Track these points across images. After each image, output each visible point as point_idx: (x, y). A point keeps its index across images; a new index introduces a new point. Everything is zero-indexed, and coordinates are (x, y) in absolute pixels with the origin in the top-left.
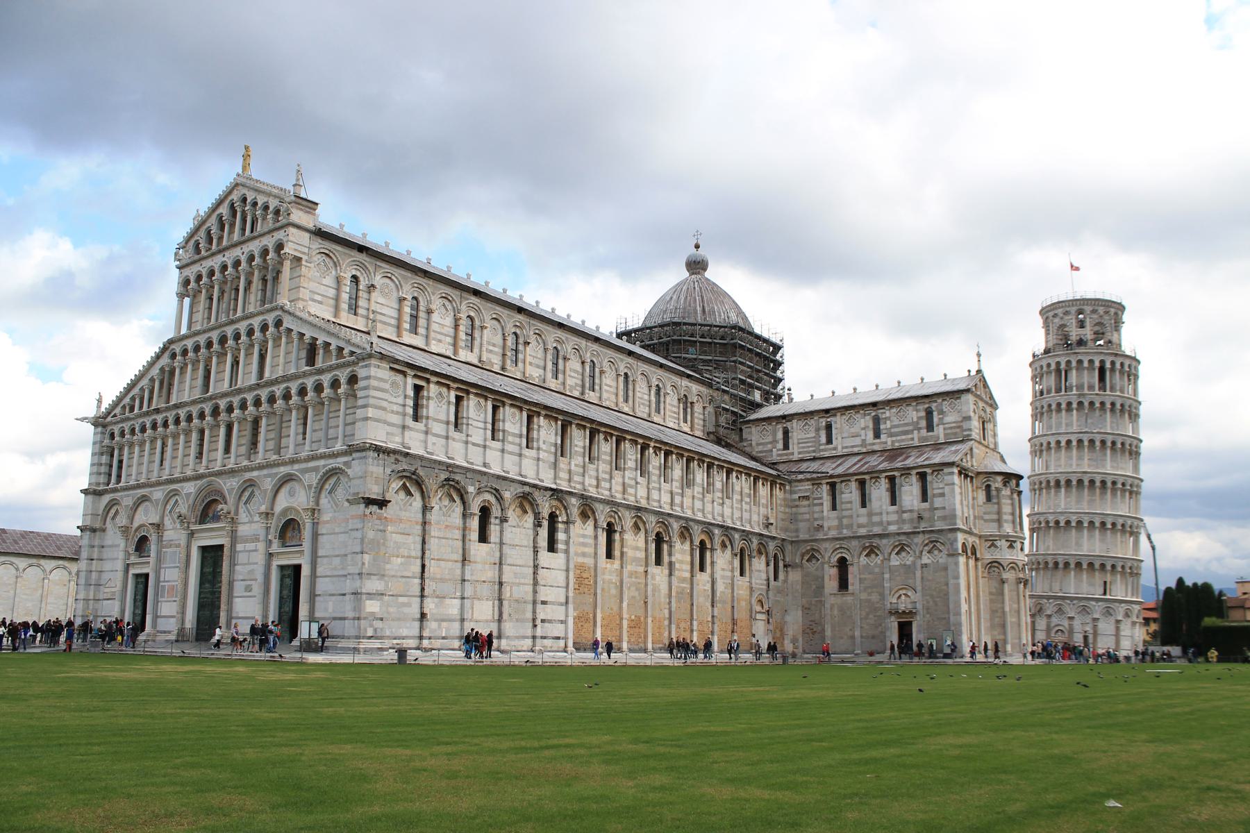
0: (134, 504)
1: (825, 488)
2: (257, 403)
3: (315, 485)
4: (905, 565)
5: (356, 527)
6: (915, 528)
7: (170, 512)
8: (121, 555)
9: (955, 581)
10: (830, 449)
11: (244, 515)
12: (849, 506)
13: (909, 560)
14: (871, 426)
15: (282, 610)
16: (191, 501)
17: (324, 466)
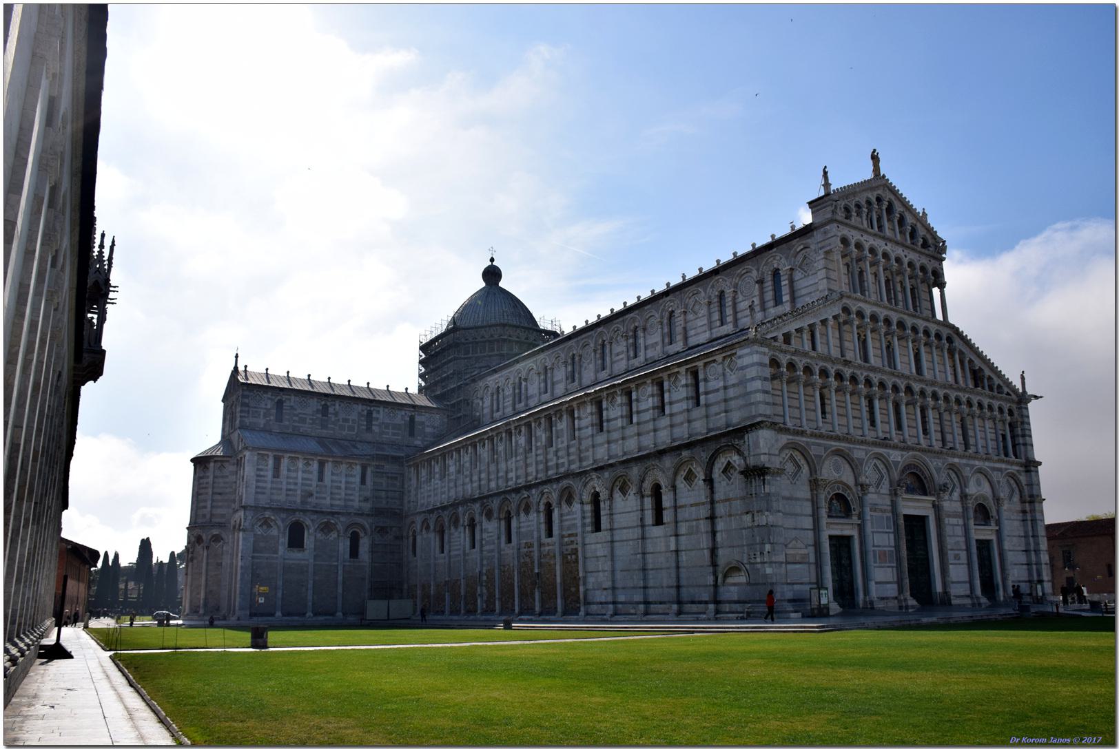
17: (1006, 469)
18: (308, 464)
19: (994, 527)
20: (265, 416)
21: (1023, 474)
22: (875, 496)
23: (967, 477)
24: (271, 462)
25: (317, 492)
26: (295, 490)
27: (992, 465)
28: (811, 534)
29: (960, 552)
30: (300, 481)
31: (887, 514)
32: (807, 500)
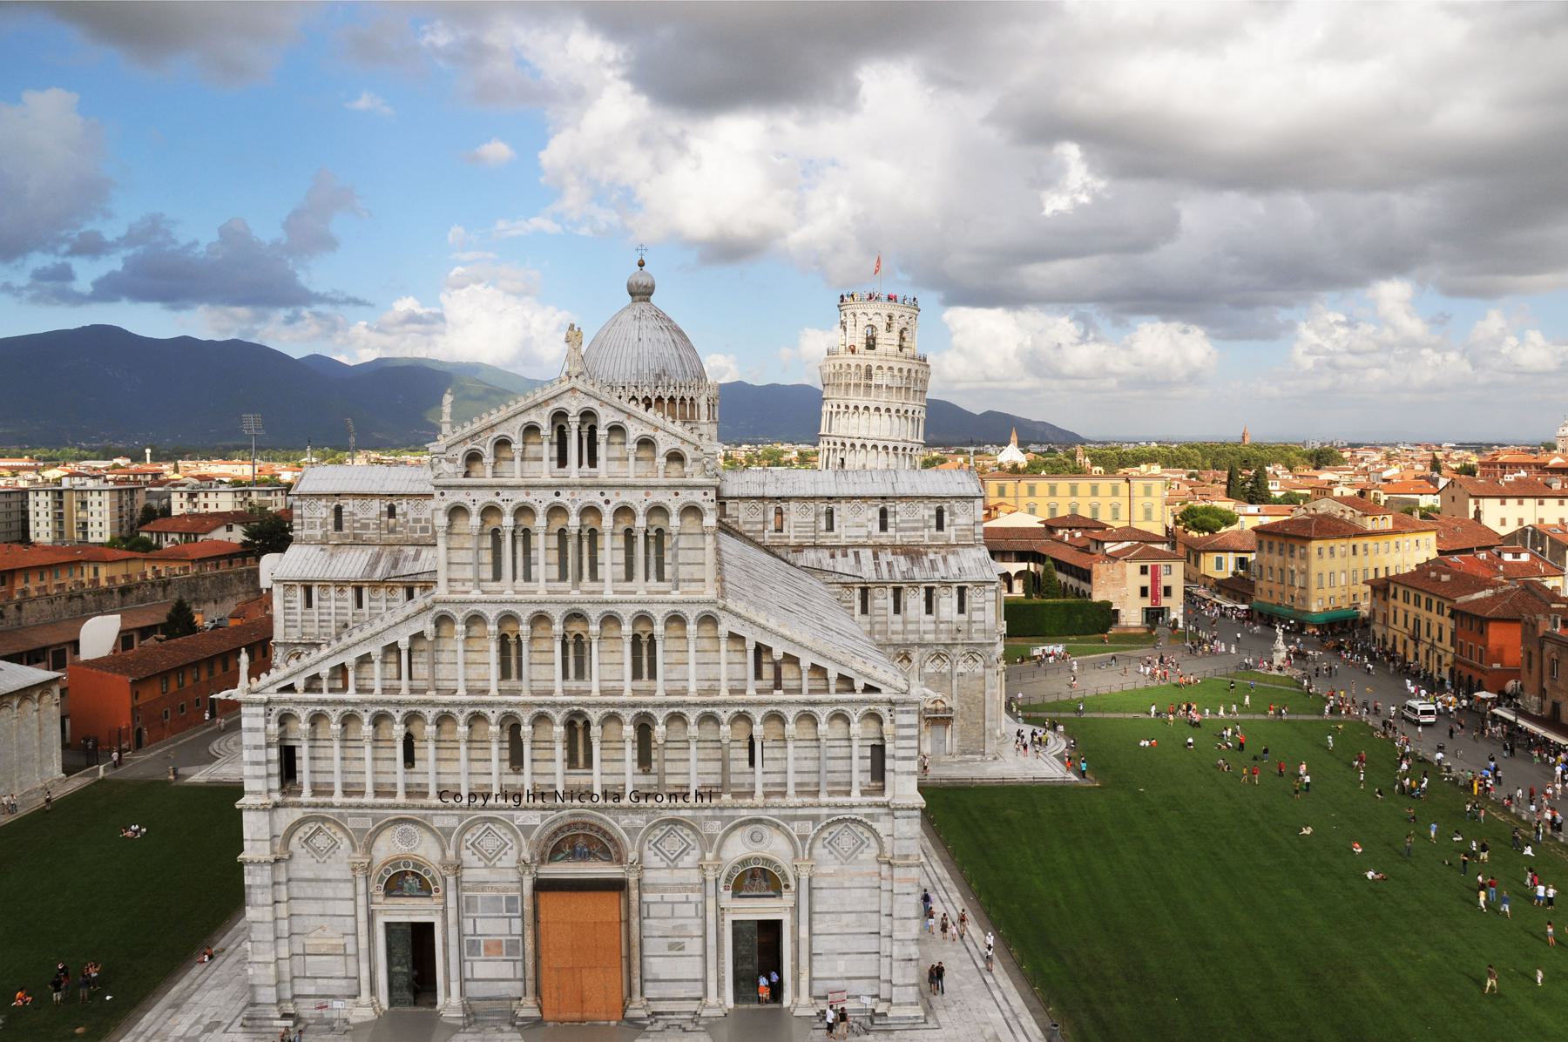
0: (378, 828)
1: (857, 592)
2: (676, 718)
3: (812, 836)
4: (940, 673)
5: (906, 891)
6: (953, 639)
7: (472, 844)
8: (362, 900)
9: (992, 691)
10: (831, 537)
11: (658, 859)
12: (883, 612)
13: (946, 668)
14: (878, 518)
15: (739, 968)
16: (534, 836)
17: (829, 816)
18: (341, 591)
19: (788, 898)
20: (322, 526)
21: (882, 818)
22: (485, 872)
23: (711, 838)
24: (300, 593)
25: (354, 622)
26: (329, 621)
27: (783, 812)
28: (350, 921)
29: (688, 939)
30: (333, 611)
31: (510, 894)
32: (349, 881)
